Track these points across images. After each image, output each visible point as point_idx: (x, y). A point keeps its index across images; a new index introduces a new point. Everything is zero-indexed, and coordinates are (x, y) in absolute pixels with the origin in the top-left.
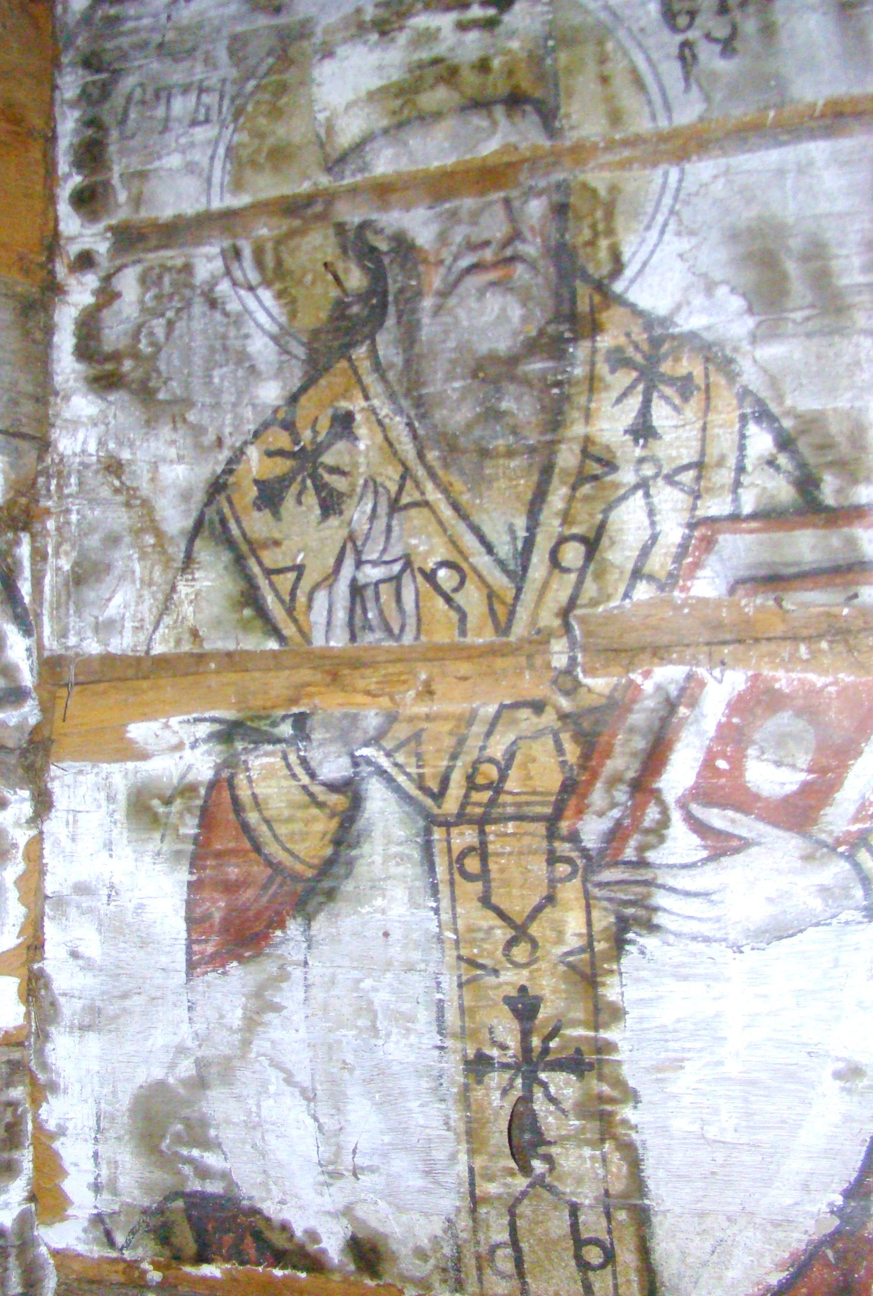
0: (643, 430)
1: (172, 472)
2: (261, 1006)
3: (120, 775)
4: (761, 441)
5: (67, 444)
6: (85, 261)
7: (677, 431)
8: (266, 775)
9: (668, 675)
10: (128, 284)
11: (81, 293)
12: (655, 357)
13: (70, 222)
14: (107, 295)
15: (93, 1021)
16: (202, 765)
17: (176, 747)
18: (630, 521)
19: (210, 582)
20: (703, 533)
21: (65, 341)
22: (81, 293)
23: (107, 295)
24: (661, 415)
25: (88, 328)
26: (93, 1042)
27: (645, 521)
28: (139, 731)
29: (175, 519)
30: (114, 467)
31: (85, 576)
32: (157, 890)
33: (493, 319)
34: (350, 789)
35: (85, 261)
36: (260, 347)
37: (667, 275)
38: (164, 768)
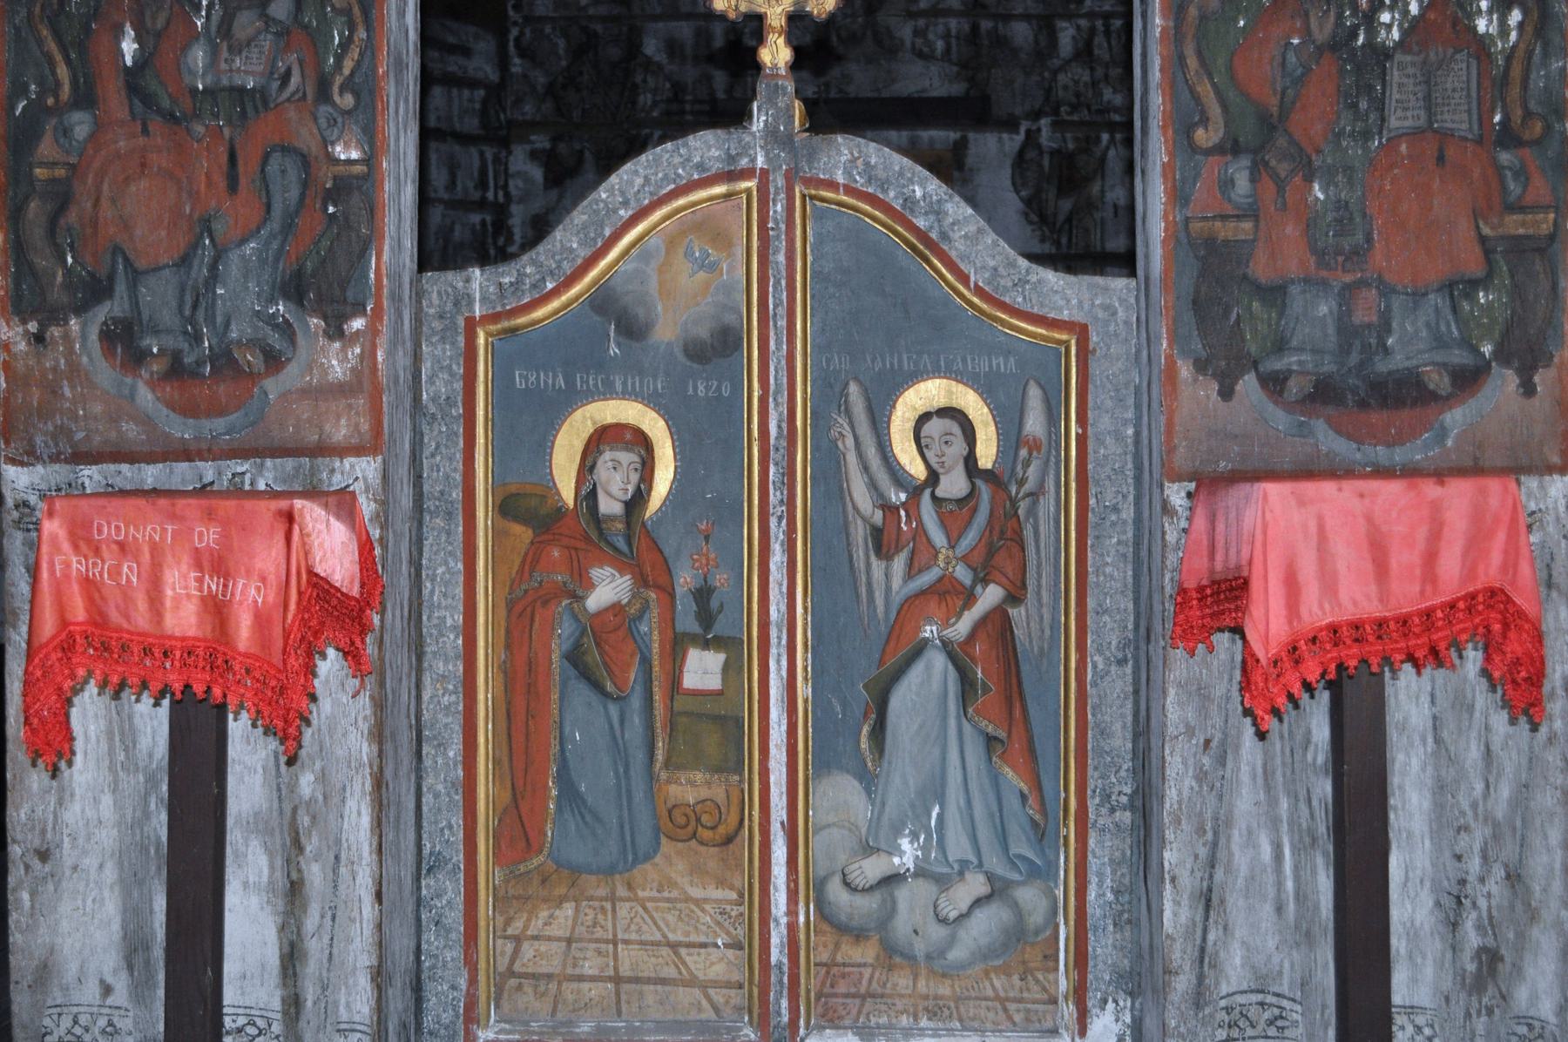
0: (645, 81)
1: (541, 79)
2: (560, 197)
3: (528, 147)
4: (668, 85)
5: (514, 70)
6: (515, 23)
7: (651, 81)
8: (562, 148)
9: (647, 131)
10: (528, 31)
11: (514, 32)
12: (648, 64)
13: (511, 13)
14: (522, 33)
15: (521, 201)
16: (547, 145)
17: (541, 141)
18: (641, 98)
19: (548, 106)
20: (655, 104)
21: (511, 44)
22: (514, 32)
23: (522, 33)
24: (649, 79)
25: (517, 40)
26: (521, 207)
27: (645, 99)
28: (533, 138)
29: (540, 88)
30: (525, 76)
31: (518, 101)
32: (537, 173)
33: (614, 52)
34: (581, 152)
35: (515, 23)
36: (561, 52)
37: (651, 47)
38: (538, 145)
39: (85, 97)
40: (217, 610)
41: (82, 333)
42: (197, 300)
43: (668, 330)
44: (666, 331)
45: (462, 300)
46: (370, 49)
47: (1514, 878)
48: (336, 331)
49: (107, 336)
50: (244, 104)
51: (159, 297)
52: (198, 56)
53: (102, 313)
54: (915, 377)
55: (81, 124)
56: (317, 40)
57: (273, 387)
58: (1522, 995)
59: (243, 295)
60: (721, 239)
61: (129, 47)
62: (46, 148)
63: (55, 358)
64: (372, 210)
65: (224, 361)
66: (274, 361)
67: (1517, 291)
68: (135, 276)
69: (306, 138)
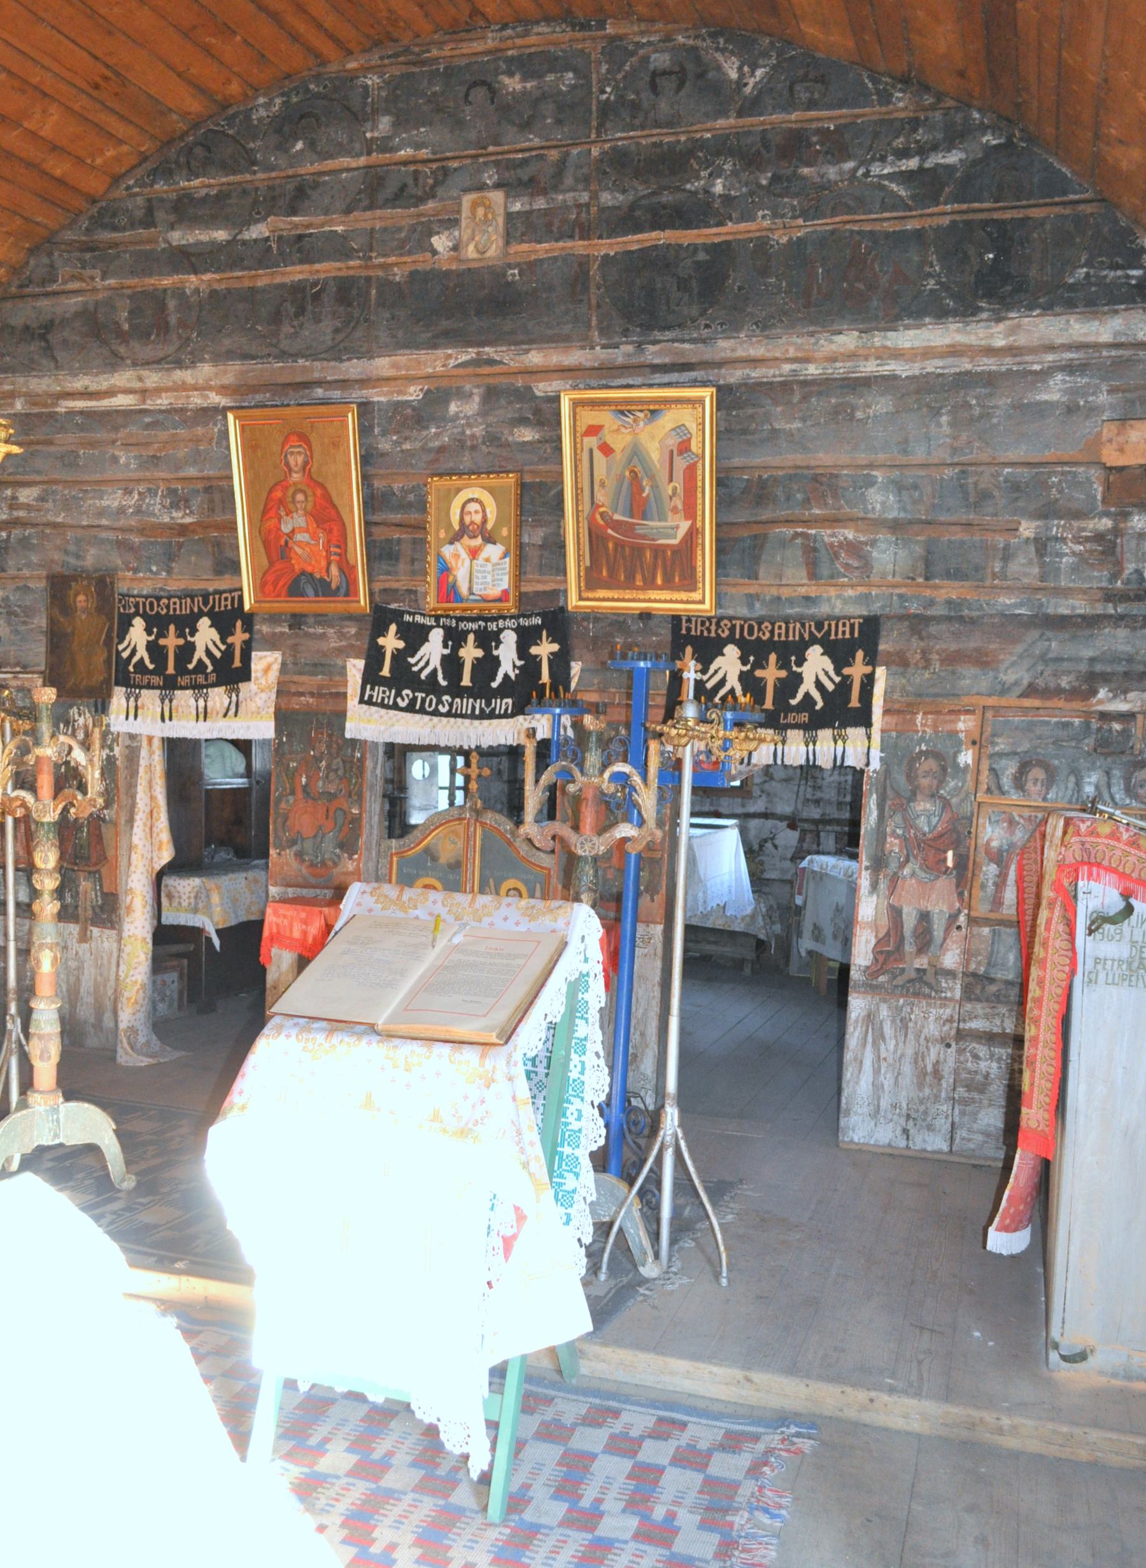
39: (293, 793)
40: (305, 933)
41: (289, 853)
42: (317, 848)
43: (443, 860)
44: (443, 860)
45: (390, 848)
46: (361, 785)
47: (642, 1035)
48: (350, 858)
49: (296, 855)
50: (331, 797)
51: (308, 845)
52: (320, 783)
53: (295, 848)
54: (507, 878)
55: (291, 799)
56: (350, 782)
57: (335, 871)
58: (642, 1067)
59: (329, 847)
60: (458, 836)
61: (304, 780)
62: (283, 805)
63: (283, 860)
64: (360, 827)
65: (323, 863)
66: (335, 864)
67: (651, 872)
68: (303, 839)
69: (345, 807)
